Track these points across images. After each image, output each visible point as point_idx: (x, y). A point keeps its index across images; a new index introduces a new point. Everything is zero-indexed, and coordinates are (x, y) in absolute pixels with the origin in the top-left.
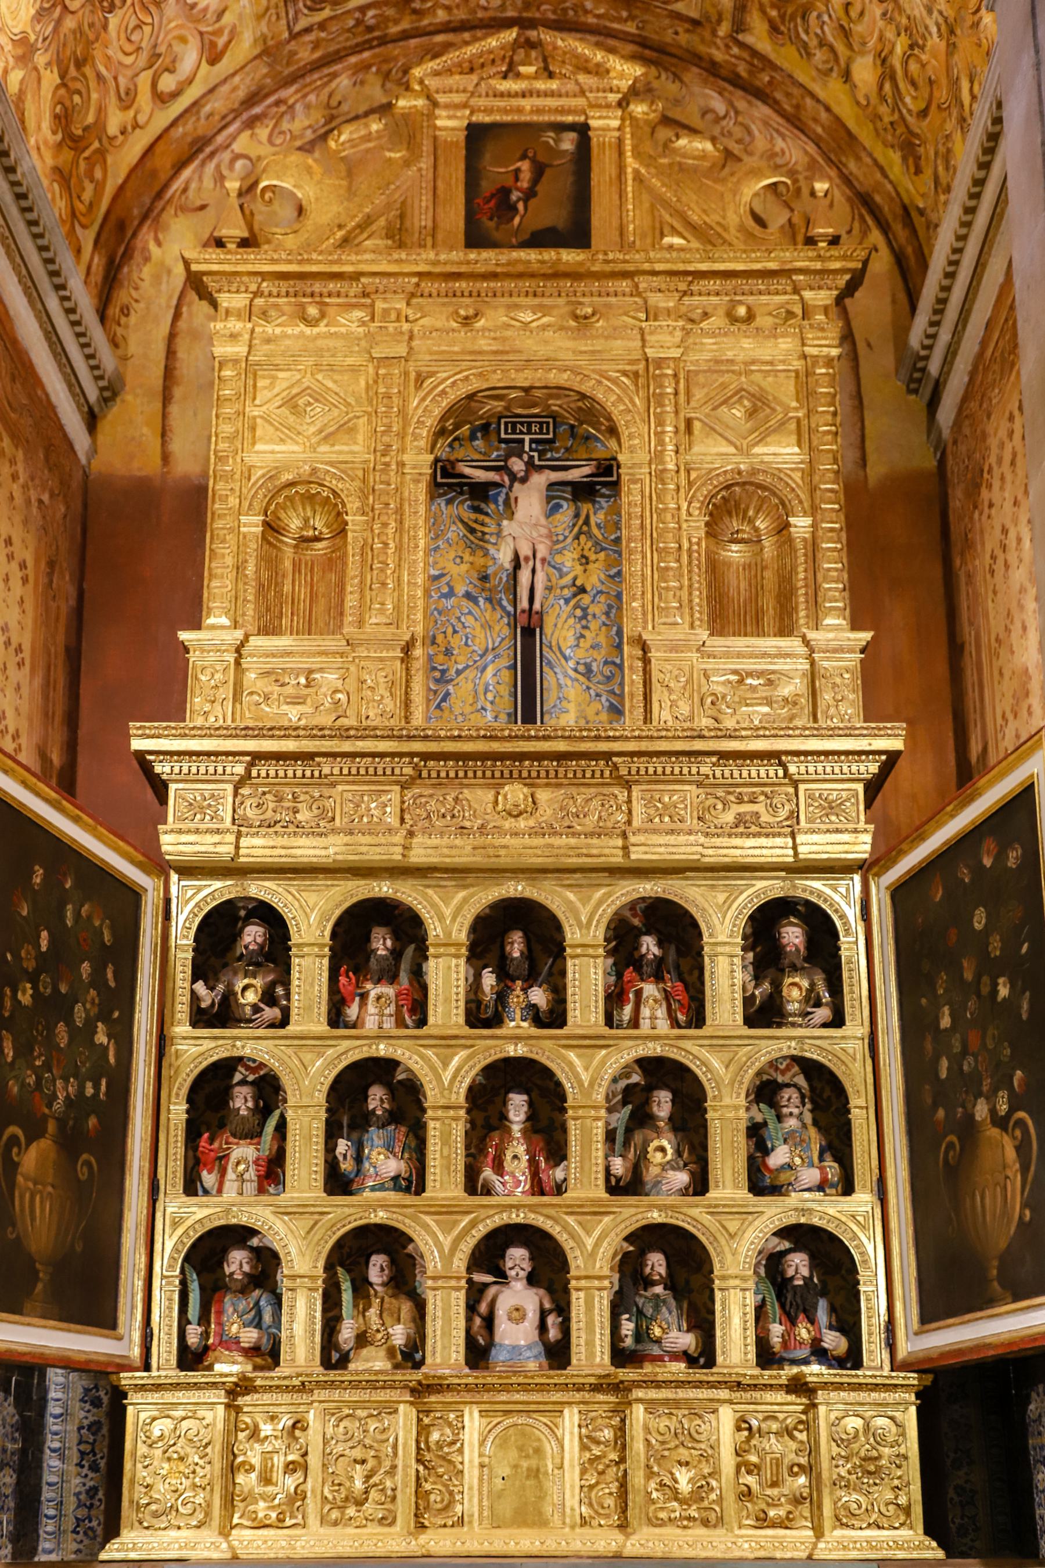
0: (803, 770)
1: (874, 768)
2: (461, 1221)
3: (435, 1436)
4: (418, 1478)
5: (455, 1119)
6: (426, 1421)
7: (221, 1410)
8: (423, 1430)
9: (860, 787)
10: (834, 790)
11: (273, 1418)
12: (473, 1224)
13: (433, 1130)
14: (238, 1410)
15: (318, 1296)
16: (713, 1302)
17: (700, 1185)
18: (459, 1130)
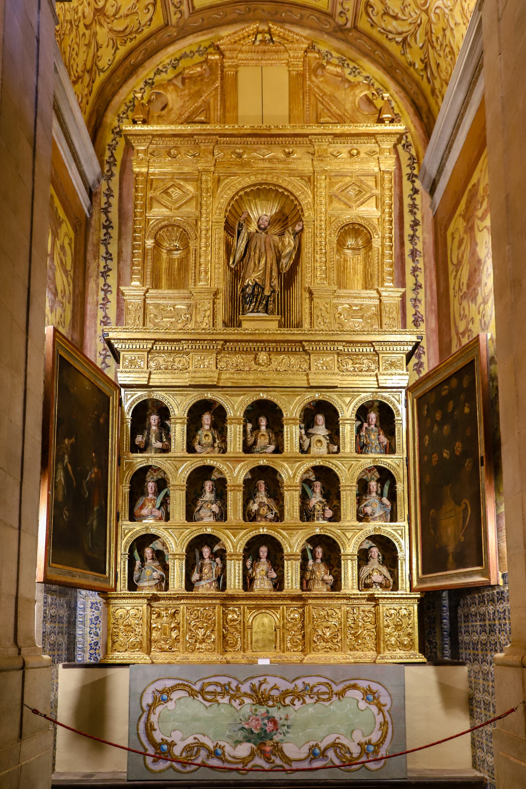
0: (381, 349)
1: (410, 348)
2: (239, 533)
3: (230, 616)
4: (223, 635)
5: (239, 491)
6: (226, 611)
7: (145, 606)
8: (225, 614)
9: (404, 356)
10: (394, 357)
11: (166, 609)
12: (246, 534)
13: (230, 495)
14: (151, 607)
15: (184, 562)
16: (341, 564)
17: (336, 518)
18: (240, 496)
